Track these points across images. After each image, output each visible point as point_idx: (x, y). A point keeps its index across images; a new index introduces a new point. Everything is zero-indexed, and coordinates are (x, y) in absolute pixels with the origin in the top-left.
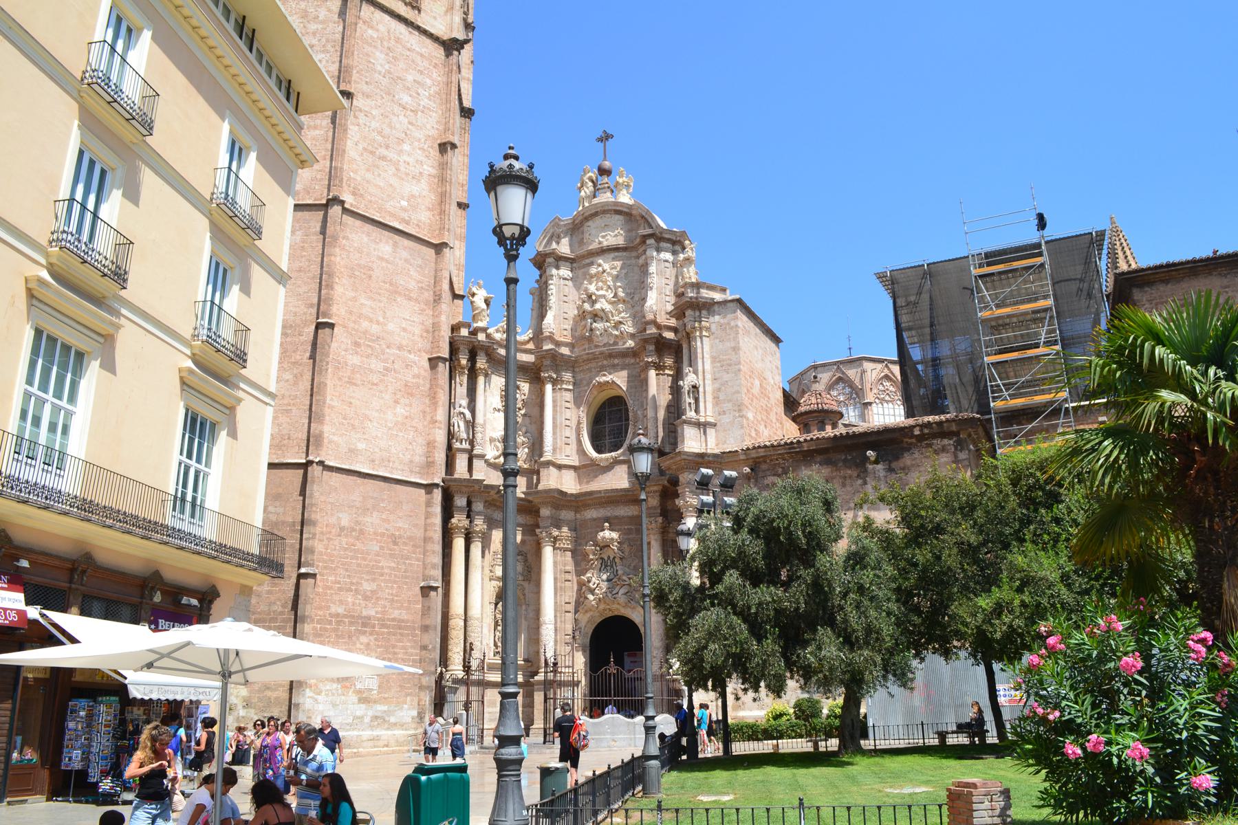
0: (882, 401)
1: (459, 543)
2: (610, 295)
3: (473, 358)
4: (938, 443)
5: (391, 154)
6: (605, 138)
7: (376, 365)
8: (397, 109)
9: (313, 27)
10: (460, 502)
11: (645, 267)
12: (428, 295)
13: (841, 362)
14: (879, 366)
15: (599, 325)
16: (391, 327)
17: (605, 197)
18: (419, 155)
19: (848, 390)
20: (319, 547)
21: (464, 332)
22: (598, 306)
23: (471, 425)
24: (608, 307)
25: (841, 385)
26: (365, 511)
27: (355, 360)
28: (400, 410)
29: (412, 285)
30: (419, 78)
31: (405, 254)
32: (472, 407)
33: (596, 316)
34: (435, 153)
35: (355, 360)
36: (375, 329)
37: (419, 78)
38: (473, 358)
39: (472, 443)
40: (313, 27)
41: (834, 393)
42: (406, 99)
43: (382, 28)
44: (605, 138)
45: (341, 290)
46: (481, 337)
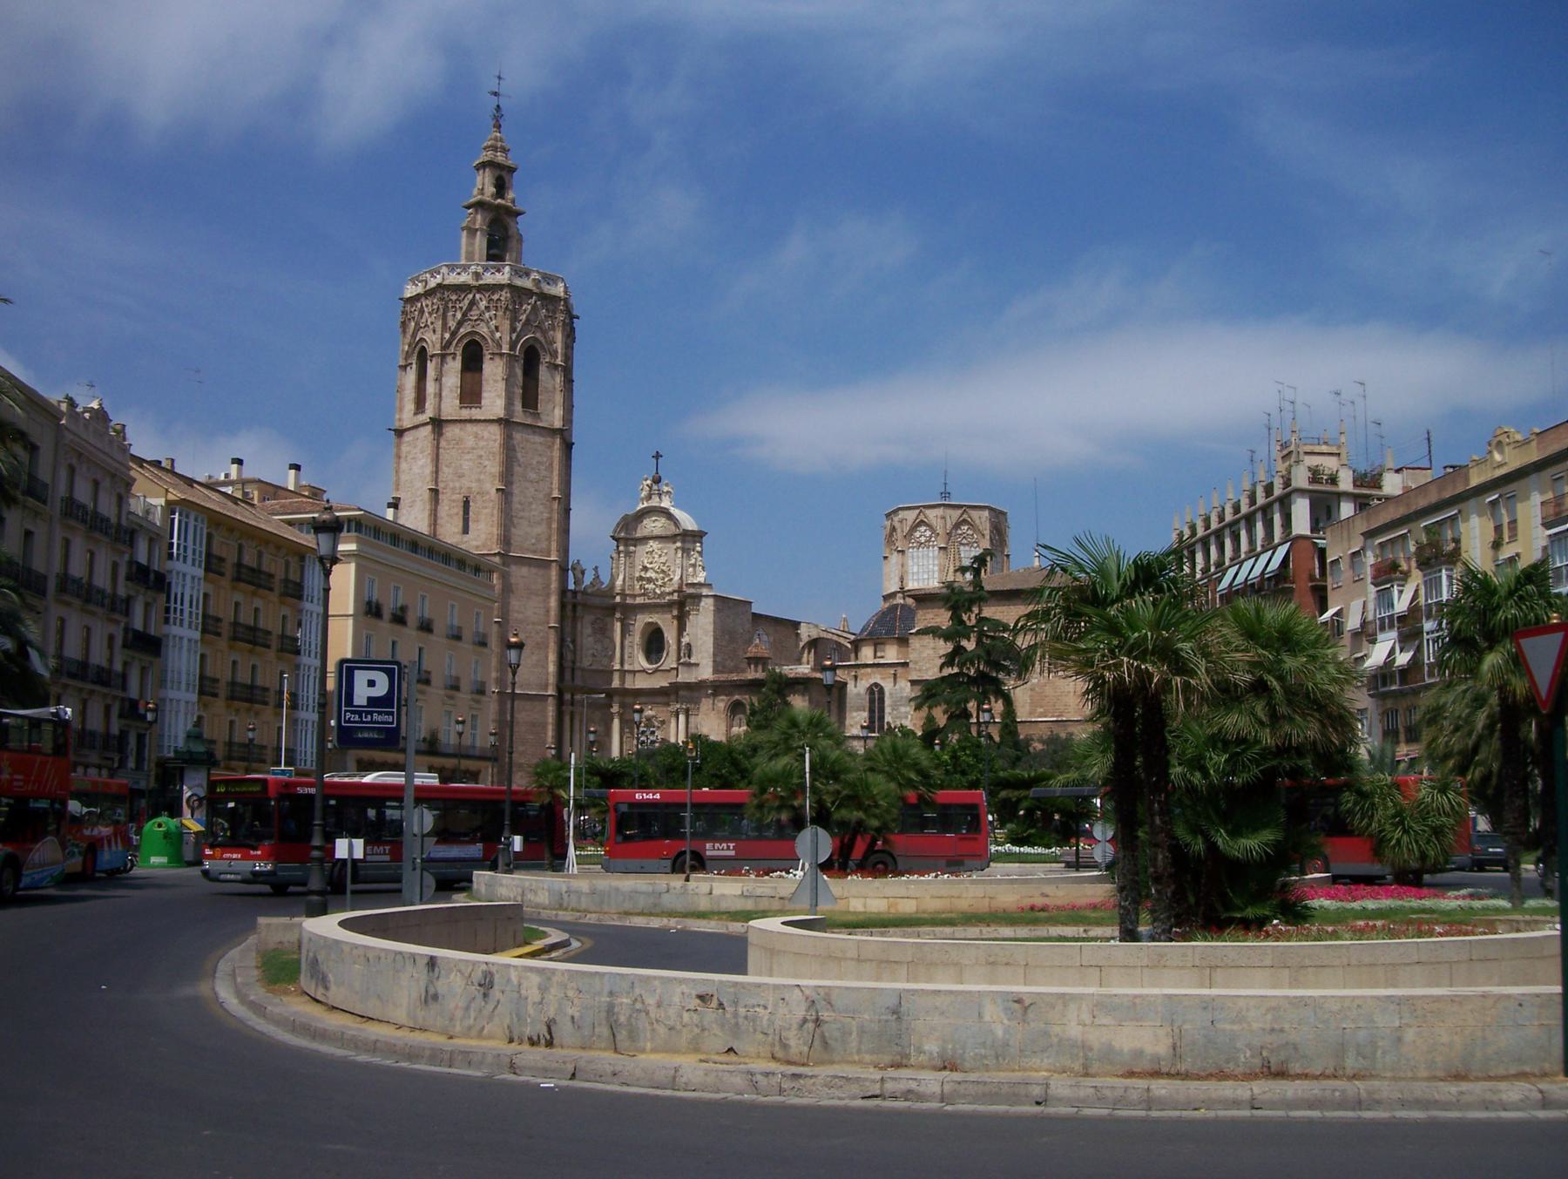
5: (526, 514)
6: (657, 456)
10: (568, 697)
14: (960, 512)
15: (651, 586)
17: (655, 502)
18: (541, 508)
21: (569, 595)
22: (648, 575)
23: (574, 652)
24: (654, 575)
25: (923, 529)
28: (534, 658)
32: (573, 642)
33: (650, 580)
36: (520, 616)
39: (574, 662)
40: (482, 443)
42: (533, 476)
44: (657, 456)
46: (579, 596)
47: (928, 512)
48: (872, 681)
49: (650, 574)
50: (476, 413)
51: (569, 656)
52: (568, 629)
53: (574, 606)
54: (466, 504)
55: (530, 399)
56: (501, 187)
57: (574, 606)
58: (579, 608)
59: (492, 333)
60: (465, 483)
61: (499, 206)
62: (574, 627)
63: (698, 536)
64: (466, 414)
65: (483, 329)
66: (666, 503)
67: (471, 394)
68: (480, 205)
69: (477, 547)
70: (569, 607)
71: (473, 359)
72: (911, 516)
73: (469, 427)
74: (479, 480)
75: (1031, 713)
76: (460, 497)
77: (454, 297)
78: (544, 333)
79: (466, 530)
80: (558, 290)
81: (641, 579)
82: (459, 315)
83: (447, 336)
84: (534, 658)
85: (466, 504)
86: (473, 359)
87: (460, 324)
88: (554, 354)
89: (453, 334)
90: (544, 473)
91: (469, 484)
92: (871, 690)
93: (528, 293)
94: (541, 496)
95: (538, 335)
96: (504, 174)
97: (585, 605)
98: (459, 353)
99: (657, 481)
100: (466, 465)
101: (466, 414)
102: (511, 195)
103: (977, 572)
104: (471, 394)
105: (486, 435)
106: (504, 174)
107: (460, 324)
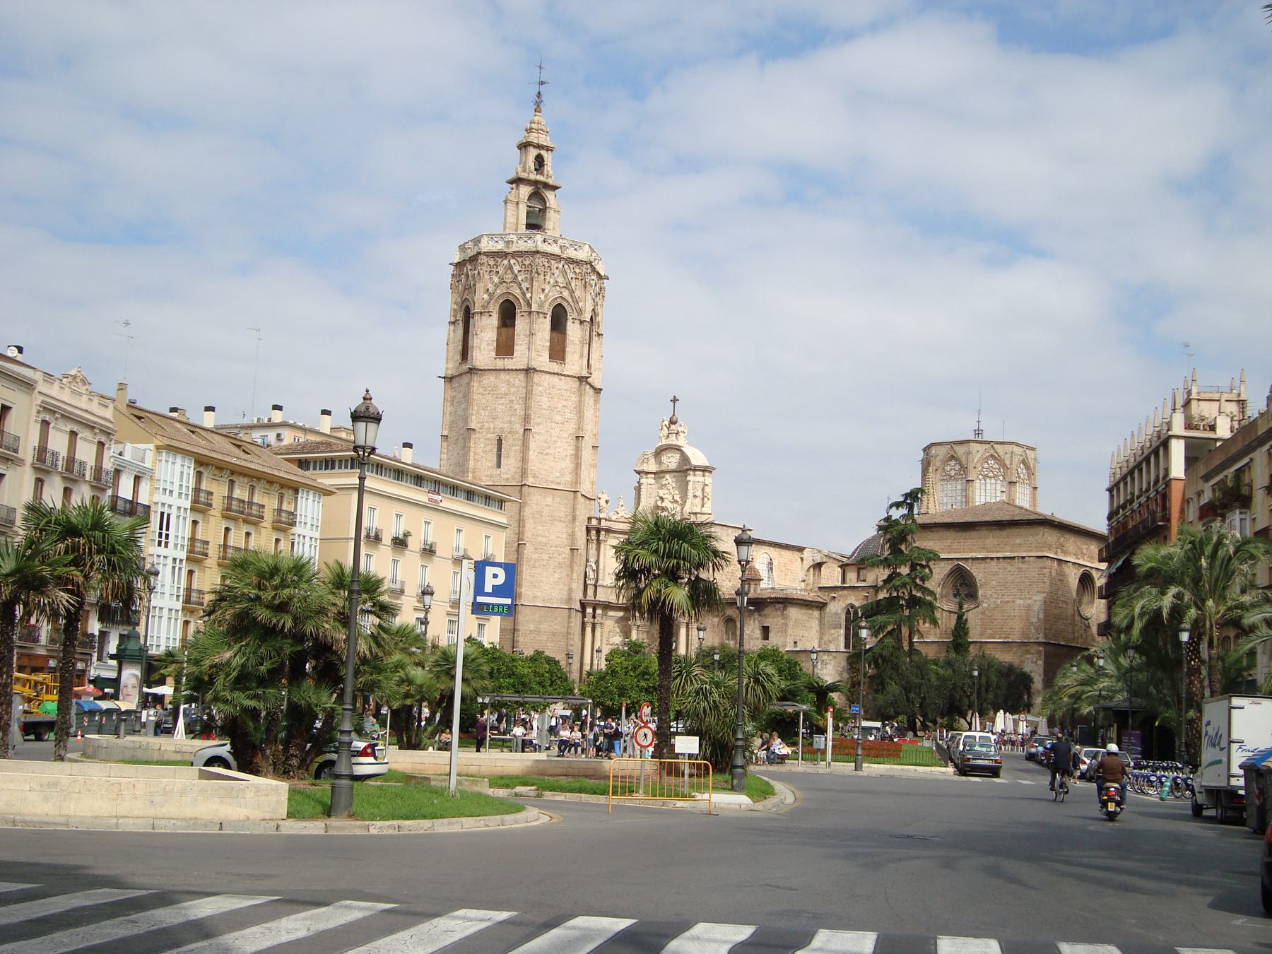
0: (985, 477)
1: (589, 630)
2: (670, 498)
3: (598, 536)
4: (778, 606)
6: (675, 400)
7: (545, 556)
8: (554, 425)
9: (513, 390)
10: (589, 610)
11: (687, 482)
12: (570, 518)
13: (954, 443)
14: (987, 446)
16: (552, 537)
17: (673, 440)
19: (957, 467)
20: (521, 639)
21: (594, 522)
23: (597, 571)
25: (952, 463)
26: (541, 623)
27: (535, 556)
28: (556, 576)
29: (562, 514)
30: (565, 403)
31: (558, 500)
32: (597, 562)
33: (663, 509)
34: (573, 442)
35: (535, 556)
36: (544, 540)
37: (565, 403)
38: (598, 536)
39: (597, 581)
40: (513, 390)
41: (948, 468)
42: (558, 418)
43: (546, 384)
44: (675, 400)
45: (529, 526)
46: (603, 523)
47: (957, 448)
48: (848, 602)
49: (667, 504)
50: (508, 363)
51: (591, 575)
52: (593, 552)
53: (598, 531)
54: (500, 441)
55: (558, 352)
56: (540, 161)
57: (598, 531)
58: (603, 533)
59: (524, 294)
60: (499, 423)
61: (536, 183)
62: (598, 549)
63: (706, 470)
64: (500, 363)
65: (517, 292)
66: (681, 441)
67: (505, 347)
68: (517, 181)
69: (507, 479)
70: (594, 532)
71: (508, 314)
72: (942, 452)
73: (503, 376)
74: (510, 422)
75: (981, 635)
76: (495, 436)
77: (492, 262)
78: (572, 292)
79: (499, 466)
80: (582, 255)
81: (657, 507)
82: (496, 280)
83: (486, 297)
84: (556, 576)
85: (500, 441)
86: (508, 314)
87: (496, 286)
88: (580, 312)
89: (491, 295)
90: (568, 415)
91: (501, 425)
92: (848, 612)
93: (559, 258)
94: (565, 435)
95: (566, 294)
96: (543, 152)
97: (608, 531)
98: (497, 308)
99: (672, 422)
100: (499, 408)
101: (500, 363)
102: (549, 167)
103: (911, 507)
104: (505, 347)
105: (517, 382)
106: (543, 152)
107: (496, 286)
